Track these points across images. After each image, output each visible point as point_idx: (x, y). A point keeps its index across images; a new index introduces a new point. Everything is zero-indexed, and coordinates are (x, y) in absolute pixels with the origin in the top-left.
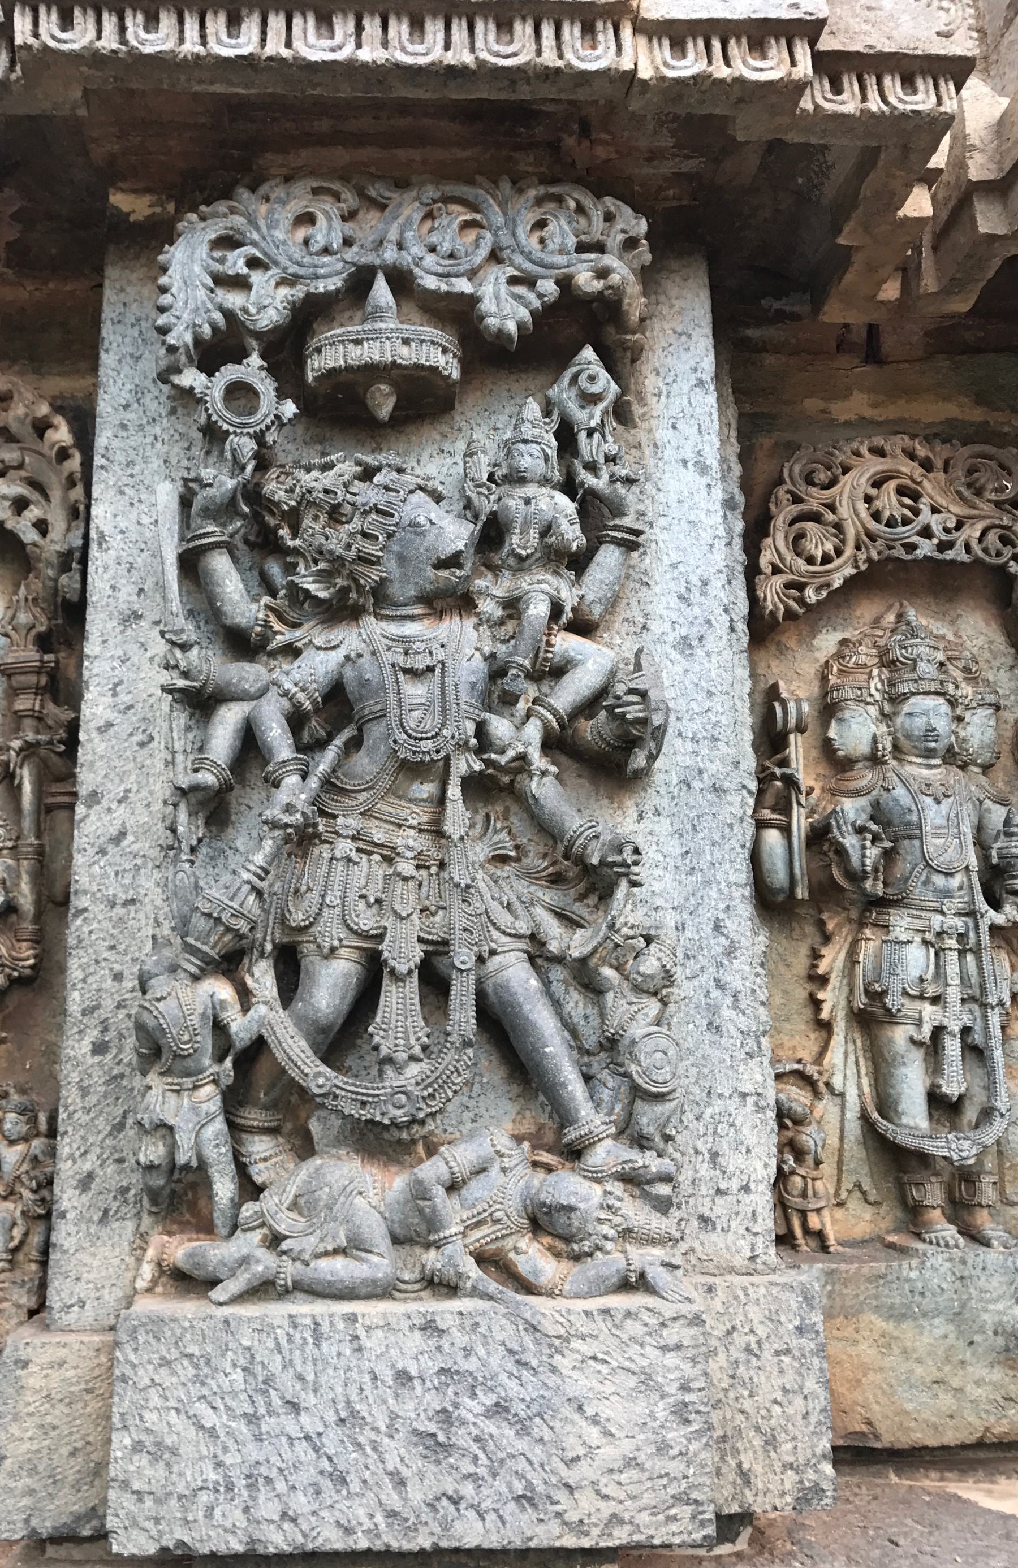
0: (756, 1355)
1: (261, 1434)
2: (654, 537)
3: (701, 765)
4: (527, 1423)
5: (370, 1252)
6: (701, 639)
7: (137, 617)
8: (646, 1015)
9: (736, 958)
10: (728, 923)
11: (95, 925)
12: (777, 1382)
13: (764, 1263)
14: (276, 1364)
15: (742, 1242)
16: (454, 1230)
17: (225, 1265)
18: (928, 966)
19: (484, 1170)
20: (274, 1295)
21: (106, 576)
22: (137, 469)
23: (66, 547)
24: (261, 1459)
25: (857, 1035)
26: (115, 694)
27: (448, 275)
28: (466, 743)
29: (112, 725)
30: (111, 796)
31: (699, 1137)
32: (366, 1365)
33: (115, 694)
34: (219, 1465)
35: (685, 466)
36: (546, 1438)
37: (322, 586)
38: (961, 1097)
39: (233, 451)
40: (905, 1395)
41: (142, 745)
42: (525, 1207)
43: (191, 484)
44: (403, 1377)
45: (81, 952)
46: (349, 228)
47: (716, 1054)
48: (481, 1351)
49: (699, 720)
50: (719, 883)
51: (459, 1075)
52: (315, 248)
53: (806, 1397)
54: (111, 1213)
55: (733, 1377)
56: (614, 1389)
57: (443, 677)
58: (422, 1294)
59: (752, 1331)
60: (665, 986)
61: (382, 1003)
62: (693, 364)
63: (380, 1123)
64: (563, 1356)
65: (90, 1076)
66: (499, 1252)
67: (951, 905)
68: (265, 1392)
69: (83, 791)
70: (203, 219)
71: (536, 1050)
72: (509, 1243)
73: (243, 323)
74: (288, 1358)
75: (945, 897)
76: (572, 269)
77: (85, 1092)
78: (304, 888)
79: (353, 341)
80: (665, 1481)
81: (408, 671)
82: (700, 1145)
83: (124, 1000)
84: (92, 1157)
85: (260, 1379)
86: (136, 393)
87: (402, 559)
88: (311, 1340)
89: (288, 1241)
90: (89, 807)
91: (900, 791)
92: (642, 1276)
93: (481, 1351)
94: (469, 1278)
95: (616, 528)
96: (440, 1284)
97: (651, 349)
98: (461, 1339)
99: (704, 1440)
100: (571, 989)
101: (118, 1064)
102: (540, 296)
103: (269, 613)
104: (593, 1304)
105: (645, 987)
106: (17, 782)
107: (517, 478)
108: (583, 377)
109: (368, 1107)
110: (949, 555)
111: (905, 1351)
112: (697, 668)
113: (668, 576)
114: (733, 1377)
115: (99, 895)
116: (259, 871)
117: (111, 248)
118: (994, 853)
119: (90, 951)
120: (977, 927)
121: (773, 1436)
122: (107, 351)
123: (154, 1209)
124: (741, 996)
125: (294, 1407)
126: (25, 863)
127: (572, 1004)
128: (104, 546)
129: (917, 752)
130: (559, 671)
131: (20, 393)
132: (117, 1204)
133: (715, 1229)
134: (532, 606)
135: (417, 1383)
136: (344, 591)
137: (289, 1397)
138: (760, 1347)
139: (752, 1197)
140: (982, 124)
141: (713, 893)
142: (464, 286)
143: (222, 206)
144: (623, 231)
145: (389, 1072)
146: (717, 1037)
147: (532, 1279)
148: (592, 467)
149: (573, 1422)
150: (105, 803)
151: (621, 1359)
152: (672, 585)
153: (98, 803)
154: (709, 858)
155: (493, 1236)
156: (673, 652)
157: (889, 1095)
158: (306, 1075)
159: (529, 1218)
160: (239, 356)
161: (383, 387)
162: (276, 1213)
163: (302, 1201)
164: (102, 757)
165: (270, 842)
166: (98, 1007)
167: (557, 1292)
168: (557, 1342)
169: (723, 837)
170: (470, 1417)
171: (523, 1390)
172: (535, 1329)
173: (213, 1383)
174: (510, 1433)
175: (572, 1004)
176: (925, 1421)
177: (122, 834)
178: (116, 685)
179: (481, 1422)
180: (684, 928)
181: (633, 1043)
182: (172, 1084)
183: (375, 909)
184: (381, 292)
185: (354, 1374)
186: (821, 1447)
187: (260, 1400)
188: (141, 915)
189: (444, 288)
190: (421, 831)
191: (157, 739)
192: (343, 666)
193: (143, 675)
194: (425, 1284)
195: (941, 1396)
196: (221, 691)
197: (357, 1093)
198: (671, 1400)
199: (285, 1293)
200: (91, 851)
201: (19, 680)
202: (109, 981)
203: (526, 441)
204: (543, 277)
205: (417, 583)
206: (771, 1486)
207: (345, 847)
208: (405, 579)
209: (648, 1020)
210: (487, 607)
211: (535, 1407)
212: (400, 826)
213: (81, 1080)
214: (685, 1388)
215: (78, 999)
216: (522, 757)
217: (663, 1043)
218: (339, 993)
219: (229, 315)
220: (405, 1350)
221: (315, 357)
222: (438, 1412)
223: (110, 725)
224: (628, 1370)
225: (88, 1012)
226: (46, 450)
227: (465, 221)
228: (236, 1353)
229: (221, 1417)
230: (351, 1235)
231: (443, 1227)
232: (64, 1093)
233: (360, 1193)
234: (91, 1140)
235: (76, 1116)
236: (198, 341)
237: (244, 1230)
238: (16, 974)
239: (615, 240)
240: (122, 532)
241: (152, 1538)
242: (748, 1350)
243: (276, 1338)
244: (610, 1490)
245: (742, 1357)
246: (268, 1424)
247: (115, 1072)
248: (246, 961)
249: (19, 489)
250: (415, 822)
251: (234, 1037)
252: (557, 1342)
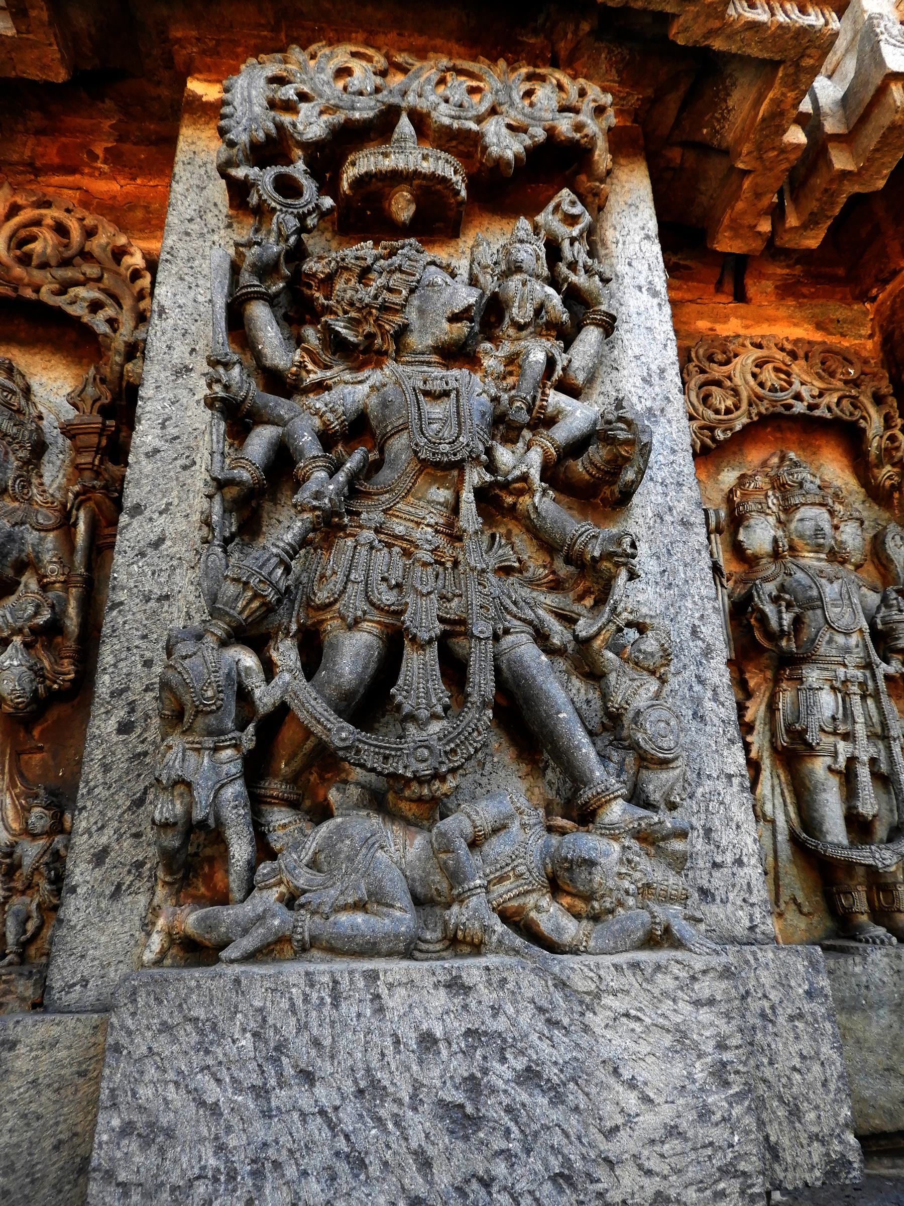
0: (771, 1021)
1: (270, 1110)
4: (561, 1090)
5: (392, 906)
6: (662, 410)
7: (188, 370)
9: (712, 658)
10: (703, 629)
11: (130, 617)
12: (794, 1048)
13: (763, 933)
14: (289, 1027)
15: (741, 913)
16: (478, 882)
17: (239, 925)
18: (837, 708)
19: (504, 827)
20: (289, 953)
21: (163, 339)
23: (132, 340)
24: (270, 1139)
25: (780, 771)
26: (163, 426)
27: (459, 118)
28: (478, 456)
29: (159, 451)
30: (154, 508)
31: (693, 814)
32: (388, 1027)
33: (163, 426)
34: (220, 1148)
35: (640, 290)
36: (582, 1106)
37: (352, 333)
38: (874, 816)
40: (862, 1083)
41: (185, 468)
42: (545, 865)
44: (428, 1041)
45: (115, 641)
47: (702, 740)
48: (510, 1010)
49: (666, 469)
50: (693, 597)
51: (480, 734)
53: (822, 1064)
55: (751, 1044)
56: (649, 1049)
57: (458, 401)
58: (444, 954)
59: (765, 996)
60: (663, 665)
61: (403, 669)
63: (402, 776)
64: (595, 1013)
65: (113, 753)
66: (520, 910)
67: (850, 660)
68: (276, 1061)
69: (128, 503)
71: (549, 716)
72: (531, 900)
73: (292, 136)
74: (303, 1020)
75: (847, 653)
76: (556, 122)
77: (106, 768)
78: (329, 573)
80: (709, 1151)
81: (426, 393)
83: (152, 684)
84: (109, 831)
85: (272, 1045)
87: (421, 312)
88: (329, 1000)
89: (307, 895)
90: (132, 517)
91: (800, 575)
92: (667, 930)
93: (510, 1010)
94: (494, 931)
96: (464, 942)
98: (488, 996)
99: (746, 1103)
100: (574, 678)
101: (143, 742)
104: (622, 959)
105: (645, 664)
106: (72, 520)
107: (515, 268)
109: (390, 761)
111: (858, 1041)
114: (751, 1044)
115: (135, 590)
116: (288, 548)
117: (186, 116)
118: (878, 621)
119: (123, 639)
120: (874, 676)
121: (796, 1105)
122: (177, 182)
123: (168, 879)
124: (720, 690)
125: (308, 1077)
126: (74, 590)
128: (164, 316)
129: (809, 548)
130: (550, 422)
131: (104, 227)
132: (131, 878)
133: (714, 900)
134: (531, 356)
135: (442, 1046)
136: (370, 337)
137: (303, 1066)
138: (774, 1012)
139: (746, 870)
140: (829, 101)
141: (689, 604)
142: (473, 126)
145: (412, 729)
146: (702, 725)
147: (555, 937)
149: (609, 1088)
150: (147, 513)
151: (654, 1016)
152: (636, 371)
153: (141, 513)
155: (515, 892)
157: (814, 818)
158: (329, 730)
159: (548, 879)
162: (295, 868)
163: (322, 857)
164: (147, 476)
165: (299, 524)
166: (127, 689)
167: (582, 949)
168: (588, 999)
169: (693, 559)
170: (500, 1084)
171: (555, 1052)
172: (564, 984)
173: (219, 1051)
174: (543, 1101)
176: (882, 1107)
177: (161, 540)
179: (512, 1088)
181: (638, 713)
182: (193, 743)
183: (395, 592)
184: (405, 126)
185: (376, 1038)
186: (843, 1115)
187: (270, 1069)
188: (174, 609)
191: (198, 464)
193: (190, 413)
194: (447, 943)
195: (893, 1082)
196: (259, 410)
197: (380, 747)
198: (709, 1059)
199: (304, 949)
200: (131, 554)
201: (83, 440)
202: (139, 666)
203: (521, 241)
205: (433, 333)
206: (799, 1160)
207: (368, 535)
208: (424, 330)
209: (650, 694)
211: (569, 1071)
213: (104, 757)
214: (721, 1046)
215: (107, 682)
216: (524, 478)
217: (665, 714)
218: (361, 663)
220: (430, 1009)
222: (465, 1079)
223: (156, 451)
224: (662, 1028)
225: (117, 694)
226: (122, 270)
228: (246, 1016)
229: (226, 1091)
230: (372, 888)
231: (466, 879)
232: (86, 769)
233: (382, 848)
234: (109, 815)
235: (97, 791)
237: (260, 889)
238: (56, 686)
239: (587, 106)
240: (180, 307)
242: (763, 1015)
243: (291, 999)
244: (653, 1164)
245: (758, 1022)
246: (280, 1098)
247: (139, 750)
248: (272, 643)
249: (96, 295)
250: (432, 521)
251: (258, 702)
252: (588, 999)
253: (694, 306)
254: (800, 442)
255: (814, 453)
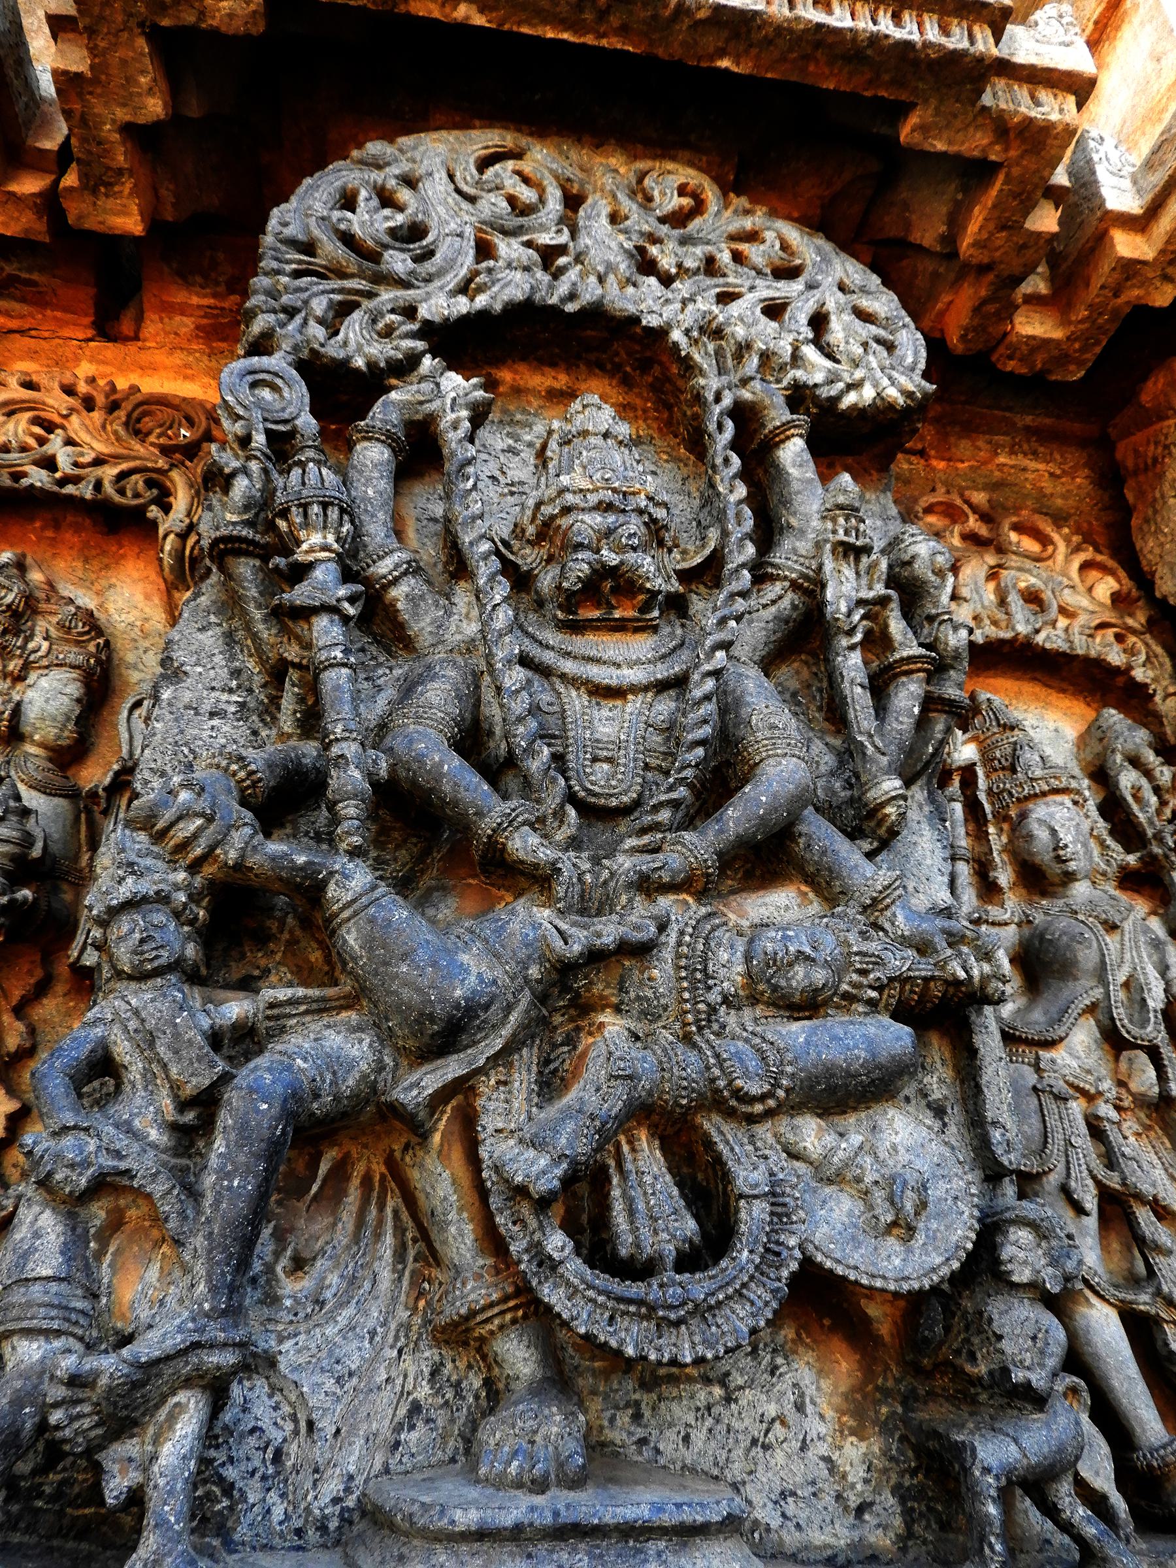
110: (70, 489)
253: (26, 342)
254: (86, 546)
255: (107, 567)
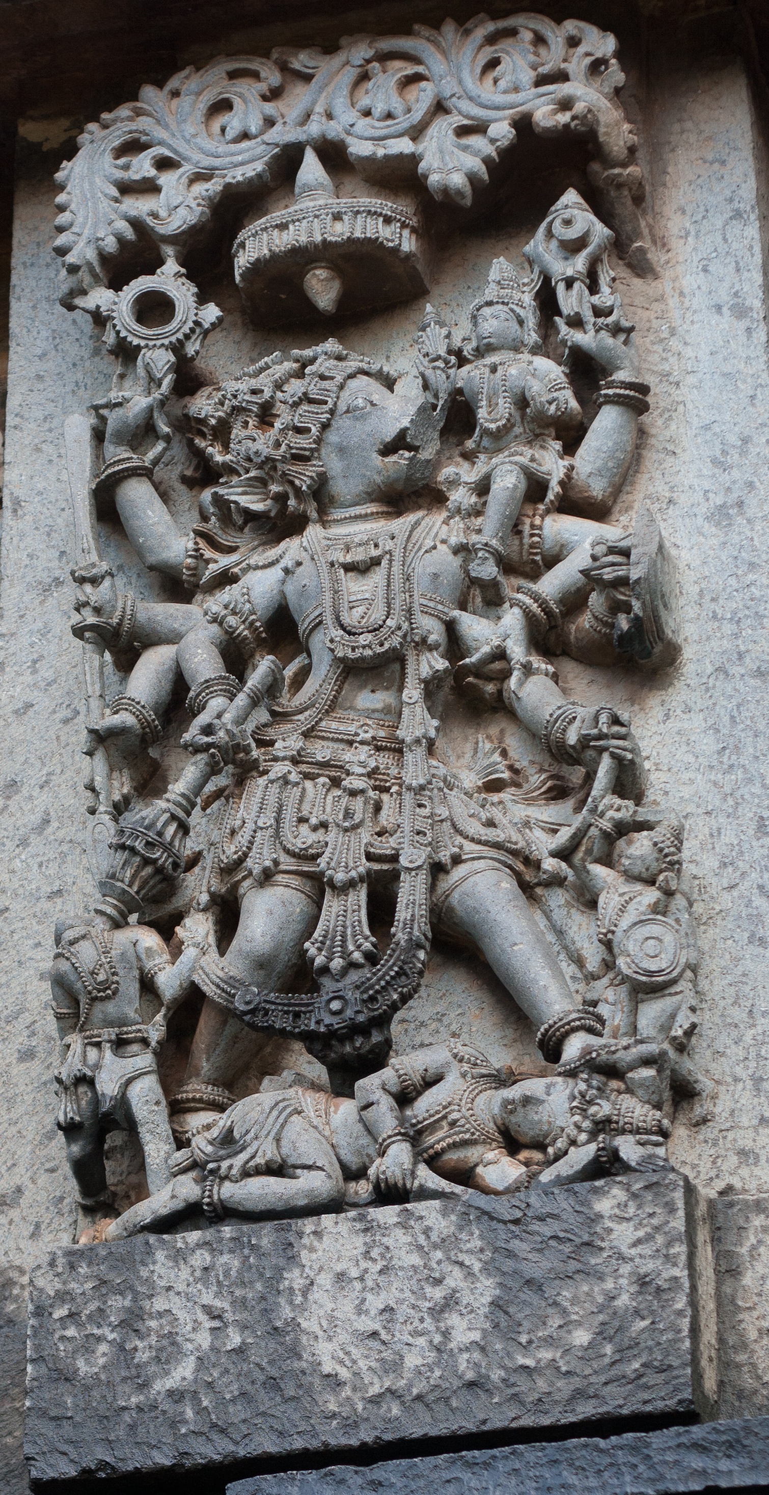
2: (680, 399)
3: (742, 648)
8: (640, 903)
22: (56, 422)
26: (35, 672)
30: (33, 782)
33: (35, 672)
39: (147, 366)
43: (101, 411)
46: (269, 108)
52: (231, 134)
54: (43, 1227)
62: (728, 193)
70: (105, 127)
79: (277, 226)
82: (739, 1071)
86: (54, 338)
95: (610, 385)
97: (674, 186)
102: (493, 141)
103: (199, 540)
108: (557, 224)
112: (736, 539)
113: (699, 440)
116: (184, 802)
127: (575, 928)
128: (20, 512)
136: (281, 499)
142: (404, 146)
143: (124, 111)
144: (588, 54)
146: (760, 950)
148: (576, 322)
150: (25, 791)
154: (751, 750)
156: (706, 525)
160: (152, 265)
161: (318, 272)
175: (575, 928)
178: (35, 662)
180: (719, 833)
189: (381, 152)
190: (378, 749)
192: (283, 582)
204: (496, 120)
210: (460, 497)
212: (350, 743)
216: (500, 655)
219: (136, 224)
221: (241, 252)
227: (406, 77)
236: (104, 258)
239: (577, 65)
240: (40, 493)
241: (72, 1461)
